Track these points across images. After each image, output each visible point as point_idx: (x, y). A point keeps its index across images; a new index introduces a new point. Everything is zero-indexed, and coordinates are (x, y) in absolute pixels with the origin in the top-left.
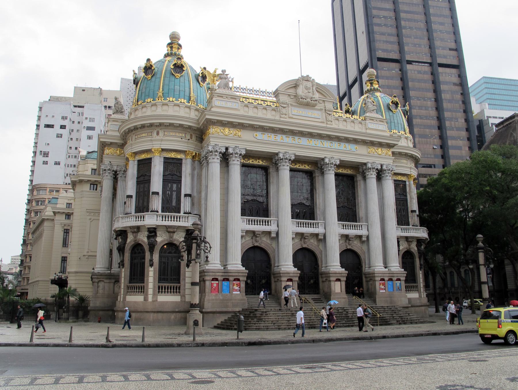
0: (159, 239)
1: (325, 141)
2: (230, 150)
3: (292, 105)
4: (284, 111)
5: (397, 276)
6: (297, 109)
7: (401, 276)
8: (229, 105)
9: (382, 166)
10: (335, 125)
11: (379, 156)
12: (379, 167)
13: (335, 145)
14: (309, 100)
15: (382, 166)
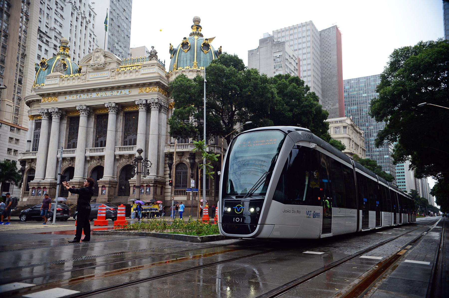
0: (26, 167)
1: (108, 92)
2: (49, 111)
3: (89, 72)
4: (83, 77)
5: (147, 183)
6: (92, 74)
7: (150, 183)
8: (53, 82)
9: (147, 101)
10: (117, 78)
11: (148, 94)
12: (144, 102)
13: (115, 93)
14: (96, 66)
15: (147, 101)
